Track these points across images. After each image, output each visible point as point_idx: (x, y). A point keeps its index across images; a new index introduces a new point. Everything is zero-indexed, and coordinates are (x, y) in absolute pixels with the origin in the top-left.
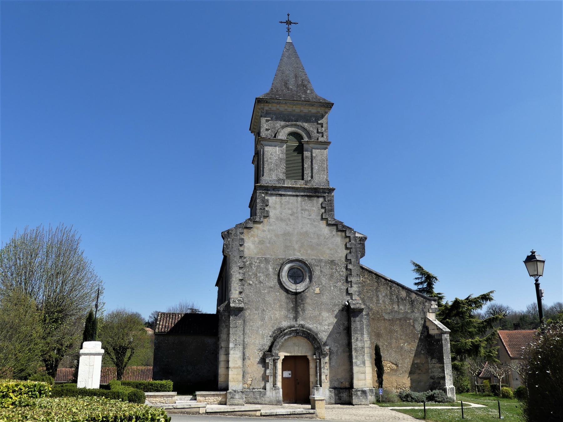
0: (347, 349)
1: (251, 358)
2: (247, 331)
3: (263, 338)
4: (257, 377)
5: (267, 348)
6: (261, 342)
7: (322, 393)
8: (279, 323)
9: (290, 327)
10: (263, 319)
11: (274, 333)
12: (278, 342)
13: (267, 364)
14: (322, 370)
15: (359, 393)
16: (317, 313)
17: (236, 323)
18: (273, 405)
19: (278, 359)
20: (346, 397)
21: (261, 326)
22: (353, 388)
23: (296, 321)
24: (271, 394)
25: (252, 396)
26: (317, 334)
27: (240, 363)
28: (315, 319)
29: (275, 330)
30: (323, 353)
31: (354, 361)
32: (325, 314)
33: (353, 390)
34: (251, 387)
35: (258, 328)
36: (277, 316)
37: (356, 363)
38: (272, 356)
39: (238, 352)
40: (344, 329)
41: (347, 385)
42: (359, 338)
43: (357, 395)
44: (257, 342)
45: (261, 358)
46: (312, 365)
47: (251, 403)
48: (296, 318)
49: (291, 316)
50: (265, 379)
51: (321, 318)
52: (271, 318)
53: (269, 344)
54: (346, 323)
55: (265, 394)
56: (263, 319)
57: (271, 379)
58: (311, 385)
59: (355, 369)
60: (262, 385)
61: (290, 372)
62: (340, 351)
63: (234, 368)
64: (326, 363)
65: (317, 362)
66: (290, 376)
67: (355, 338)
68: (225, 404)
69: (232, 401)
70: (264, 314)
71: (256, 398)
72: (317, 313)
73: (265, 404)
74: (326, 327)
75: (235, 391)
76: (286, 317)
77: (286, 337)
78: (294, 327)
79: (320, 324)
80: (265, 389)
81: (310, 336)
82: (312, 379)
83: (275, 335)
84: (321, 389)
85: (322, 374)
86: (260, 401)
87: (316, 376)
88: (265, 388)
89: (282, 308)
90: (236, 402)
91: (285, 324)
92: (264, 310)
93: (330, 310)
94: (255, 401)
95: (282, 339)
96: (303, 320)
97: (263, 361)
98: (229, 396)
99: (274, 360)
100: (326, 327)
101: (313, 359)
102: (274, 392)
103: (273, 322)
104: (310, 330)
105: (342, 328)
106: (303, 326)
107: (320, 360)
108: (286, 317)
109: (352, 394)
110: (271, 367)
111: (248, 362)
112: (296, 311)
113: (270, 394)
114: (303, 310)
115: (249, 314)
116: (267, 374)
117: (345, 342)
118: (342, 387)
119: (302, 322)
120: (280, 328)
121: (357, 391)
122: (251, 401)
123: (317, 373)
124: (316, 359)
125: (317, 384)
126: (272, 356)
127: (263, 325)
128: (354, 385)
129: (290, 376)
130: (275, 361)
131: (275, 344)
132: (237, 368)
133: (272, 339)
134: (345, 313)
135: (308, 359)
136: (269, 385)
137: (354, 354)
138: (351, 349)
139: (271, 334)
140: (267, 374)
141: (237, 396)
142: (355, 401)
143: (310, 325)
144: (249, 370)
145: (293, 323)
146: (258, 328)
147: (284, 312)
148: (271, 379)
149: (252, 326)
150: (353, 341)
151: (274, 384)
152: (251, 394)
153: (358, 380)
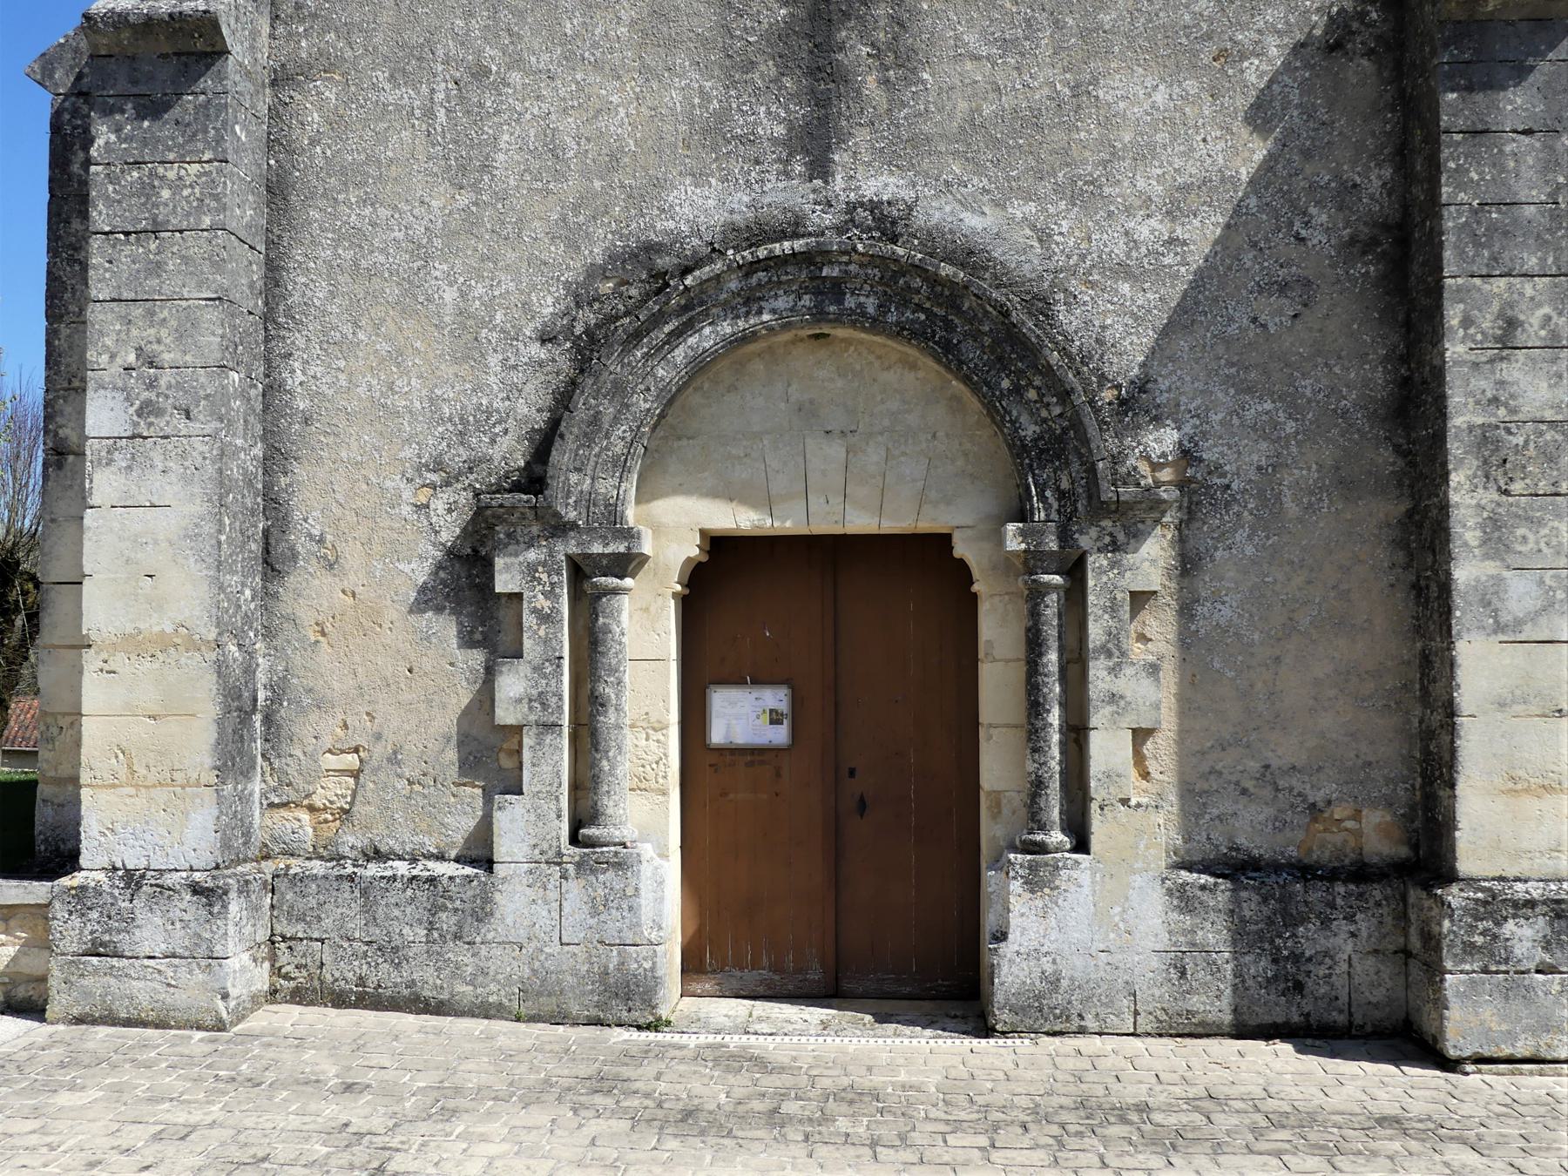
0: (1385, 458)
1: (352, 555)
2: (308, 285)
3: (470, 352)
4: (412, 748)
5: (510, 452)
6: (455, 397)
7: (1100, 912)
8: (636, 199)
9: (757, 233)
10: (467, 167)
11: (580, 297)
12: (619, 390)
13: (506, 614)
14: (1098, 671)
15: (1523, 936)
16: (1046, 78)
17: (147, 190)
18: (559, 1018)
19: (627, 564)
20: (1366, 968)
21: (450, 235)
22: (1449, 876)
23: (820, 168)
24: (544, 916)
25: (356, 926)
26: (1041, 305)
27: (187, 597)
28: (1012, 142)
29: (595, 272)
30: (1107, 493)
31: (1466, 572)
32: (1136, 93)
33: (1455, 896)
34: (351, 840)
35: (420, 252)
36: (618, 125)
37: (1489, 597)
38: (560, 529)
39: (167, 488)
40: (1356, 247)
41: (1375, 833)
42: (1533, 327)
43: (1493, 956)
44: (412, 390)
45: (452, 554)
46: (997, 629)
47: (339, 1000)
48: (814, 146)
49: (770, 122)
50: (490, 757)
51: (1089, 131)
52: (555, 152)
53: (530, 408)
54: (1376, 179)
55: (482, 912)
56: (467, 167)
57: (546, 766)
58: (991, 831)
59: (1480, 666)
60: (461, 824)
61: (776, 698)
62: (1303, 471)
63: (136, 644)
64: (1140, 599)
65: (1036, 594)
66: (780, 735)
67: (1488, 322)
68: (33, 1009)
69: (99, 981)
70: (478, 116)
71: (393, 953)
72: (1046, 78)
73: (485, 1011)
74: (1148, 229)
75: (132, 880)
76: (714, 134)
77: (706, 337)
78: (795, 228)
79: (1084, 194)
80: (488, 864)
81: (968, 327)
82: (997, 768)
83: (588, 317)
84: (1080, 874)
85: (1098, 718)
86: (428, 979)
87: (1034, 735)
88: (480, 854)
89: (671, 44)
90: (141, 990)
91: (698, 206)
92: (480, 73)
93: (1202, 51)
94: (385, 976)
95: (660, 352)
96: (890, 159)
97: (466, 585)
98: (70, 931)
99: (579, 570)
100: (1148, 229)
101: (1005, 564)
102: (574, 888)
103: (571, 186)
104: (969, 256)
105: (1323, 227)
106: (886, 221)
107: (1075, 571)
108: (714, 134)
109: (1432, 942)
110: (547, 631)
111: (311, 593)
112: (814, 72)
113: (532, 909)
114: (900, 60)
115: (336, 122)
116: (506, 715)
117: (1362, 376)
118: (1321, 855)
119: (881, 185)
120: (650, 248)
121: (1497, 905)
122: (343, 972)
123: (1035, 707)
124: (1032, 561)
125: (1036, 820)
126: (560, 529)
127: (471, 222)
128: (1464, 839)
129: (780, 735)
130: (590, 583)
131: (582, 406)
132: (164, 643)
133: (561, 359)
134: (1360, 71)
135: (962, 572)
136: (527, 826)
137: (1466, 495)
138: (1439, 438)
139: (548, 306)
140: (506, 715)
141: (151, 932)
142: (1467, 1015)
143: (966, 209)
144: (328, 669)
145: (785, 193)
146: (420, 252)
147: (687, 87)
148: (546, 766)
149: (356, 238)
150: (1455, 349)
151: (584, 816)
152: (344, 911)
153: (1515, 786)
